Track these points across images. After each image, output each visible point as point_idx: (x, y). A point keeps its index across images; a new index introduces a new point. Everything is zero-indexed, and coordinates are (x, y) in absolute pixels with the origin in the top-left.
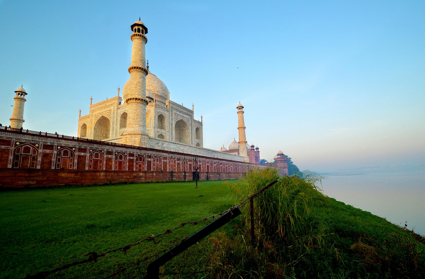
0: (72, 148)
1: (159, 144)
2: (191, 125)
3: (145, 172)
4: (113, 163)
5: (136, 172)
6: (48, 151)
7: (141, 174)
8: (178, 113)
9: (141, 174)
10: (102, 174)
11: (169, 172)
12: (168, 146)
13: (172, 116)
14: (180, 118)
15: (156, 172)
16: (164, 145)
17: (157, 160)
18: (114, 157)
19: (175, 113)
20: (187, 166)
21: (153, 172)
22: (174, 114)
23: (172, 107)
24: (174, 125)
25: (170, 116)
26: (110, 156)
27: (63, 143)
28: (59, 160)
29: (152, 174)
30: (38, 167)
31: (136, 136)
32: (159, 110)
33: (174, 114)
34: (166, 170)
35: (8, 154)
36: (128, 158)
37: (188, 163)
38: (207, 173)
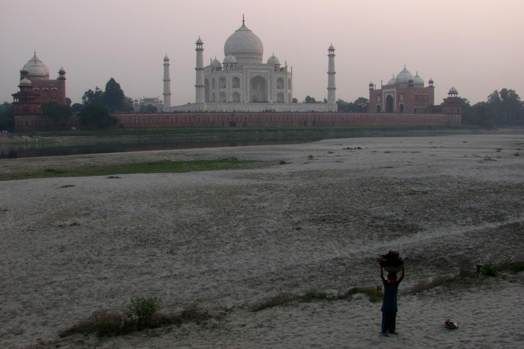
8: (254, 71)
14: (255, 75)
23: (246, 68)
27: (166, 114)
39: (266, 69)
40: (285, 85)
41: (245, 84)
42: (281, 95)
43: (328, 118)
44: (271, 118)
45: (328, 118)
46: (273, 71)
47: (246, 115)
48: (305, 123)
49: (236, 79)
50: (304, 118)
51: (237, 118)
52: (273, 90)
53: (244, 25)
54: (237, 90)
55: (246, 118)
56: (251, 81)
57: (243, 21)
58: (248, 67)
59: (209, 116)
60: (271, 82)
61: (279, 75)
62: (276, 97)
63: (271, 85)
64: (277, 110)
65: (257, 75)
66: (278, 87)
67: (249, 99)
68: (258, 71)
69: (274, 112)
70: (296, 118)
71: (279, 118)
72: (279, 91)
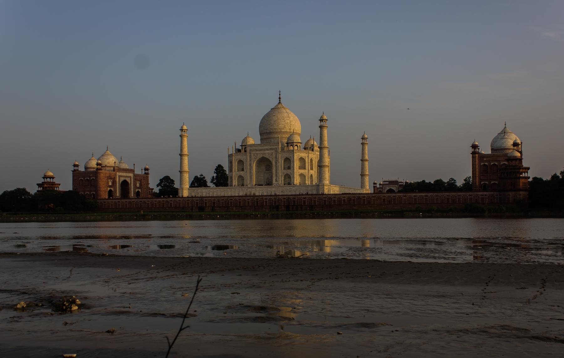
2: (276, 158)
8: (257, 152)
14: (260, 156)
39: (271, 149)
40: (292, 165)
41: (249, 167)
44: (240, 202)
45: (304, 202)
47: (214, 200)
48: (277, 208)
49: (241, 162)
50: (275, 202)
51: (206, 203)
54: (242, 173)
55: (214, 203)
57: (280, 98)
58: (251, 148)
60: (276, 163)
63: (276, 167)
64: (257, 194)
65: (261, 156)
66: (289, 168)
68: (262, 152)
69: (254, 196)
70: (266, 202)
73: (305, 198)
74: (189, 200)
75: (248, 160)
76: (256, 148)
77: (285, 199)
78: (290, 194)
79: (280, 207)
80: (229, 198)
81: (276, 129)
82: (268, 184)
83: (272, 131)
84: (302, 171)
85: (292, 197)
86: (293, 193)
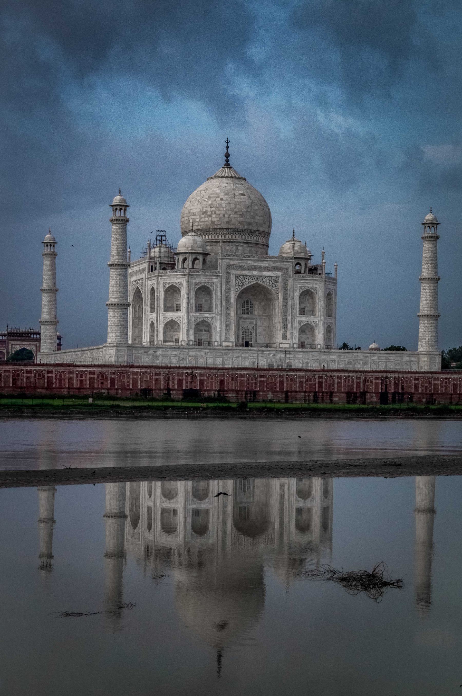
0: (43, 371)
1: (149, 353)
2: (285, 288)
3: (108, 389)
4: (75, 381)
5: (97, 389)
6: (29, 375)
7: (103, 391)
9: (103, 391)
10: (65, 390)
11: (141, 390)
12: (164, 353)
13: (228, 282)
14: (249, 283)
15: (121, 389)
16: (158, 353)
17: (124, 376)
18: (75, 376)
19: (237, 276)
20: (173, 383)
21: (117, 389)
22: (233, 278)
23: (229, 266)
24: (233, 300)
25: (224, 283)
26: (71, 376)
28: (35, 380)
29: (115, 391)
30: (25, 385)
31: (112, 348)
32: (197, 280)
33: (233, 278)
34: (137, 386)
35: (9, 378)
36: (88, 376)
37: (176, 378)
38: (219, 391)
41: (224, 304)
42: (307, 329)
43: (416, 387)
44: (282, 383)
45: (416, 387)
46: (291, 272)
47: (223, 375)
50: (358, 384)
51: (202, 382)
52: (289, 318)
53: (227, 165)
56: (239, 297)
57: (227, 156)
58: (232, 262)
59: (137, 374)
61: (306, 282)
62: (296, 334)
66: (302, 312)
67: (233, 338)
68: (255, 273)
71: (301, 383)
72: (304, 319)
73: (418, 379)
74: (160, 374)
75: (224, 289)
76: (243, 263)
77: (377, 378)
78: (366, 368)
79: (368, 395)
80: (259, 373)
81: (249, 224)
82: (247, 344)
83: (241, 227)
84: (329, 320)
85: (393, 375)
86: (374, 368)
